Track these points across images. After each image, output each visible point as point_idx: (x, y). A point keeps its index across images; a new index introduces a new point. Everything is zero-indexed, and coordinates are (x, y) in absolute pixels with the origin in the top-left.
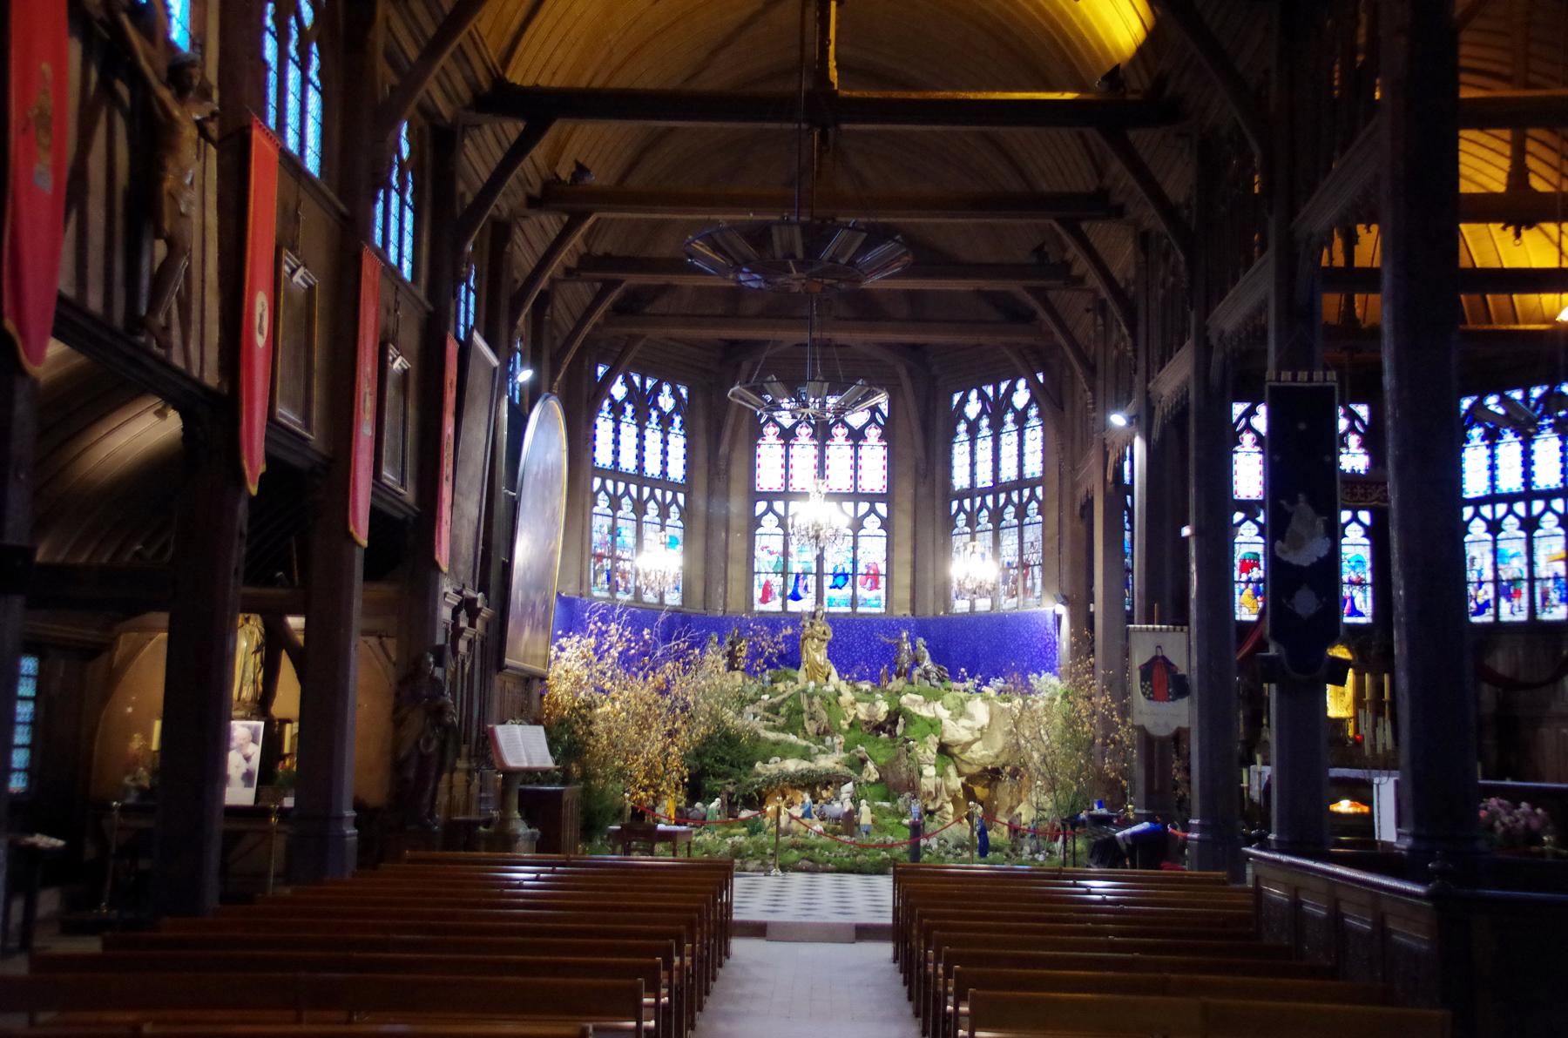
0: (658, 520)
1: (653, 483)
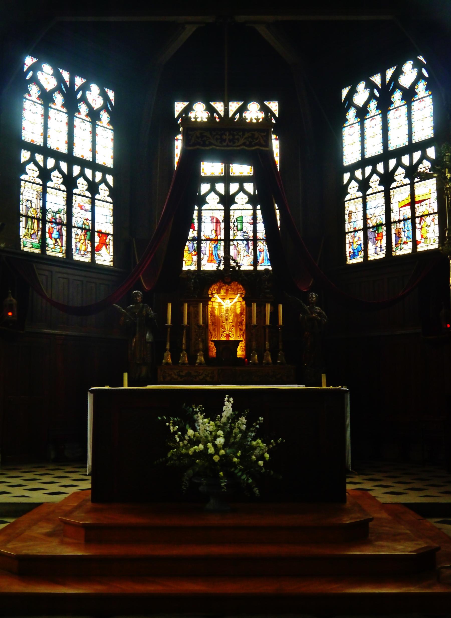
0: (88, 194)
1: (83, 163)
